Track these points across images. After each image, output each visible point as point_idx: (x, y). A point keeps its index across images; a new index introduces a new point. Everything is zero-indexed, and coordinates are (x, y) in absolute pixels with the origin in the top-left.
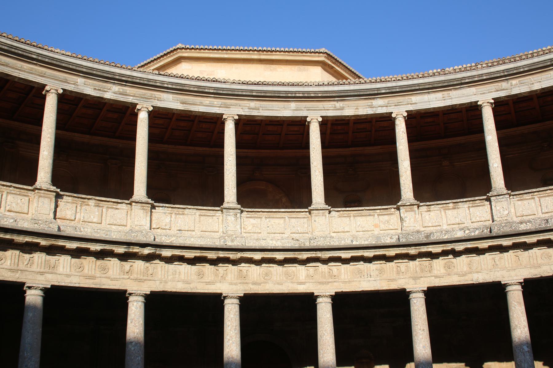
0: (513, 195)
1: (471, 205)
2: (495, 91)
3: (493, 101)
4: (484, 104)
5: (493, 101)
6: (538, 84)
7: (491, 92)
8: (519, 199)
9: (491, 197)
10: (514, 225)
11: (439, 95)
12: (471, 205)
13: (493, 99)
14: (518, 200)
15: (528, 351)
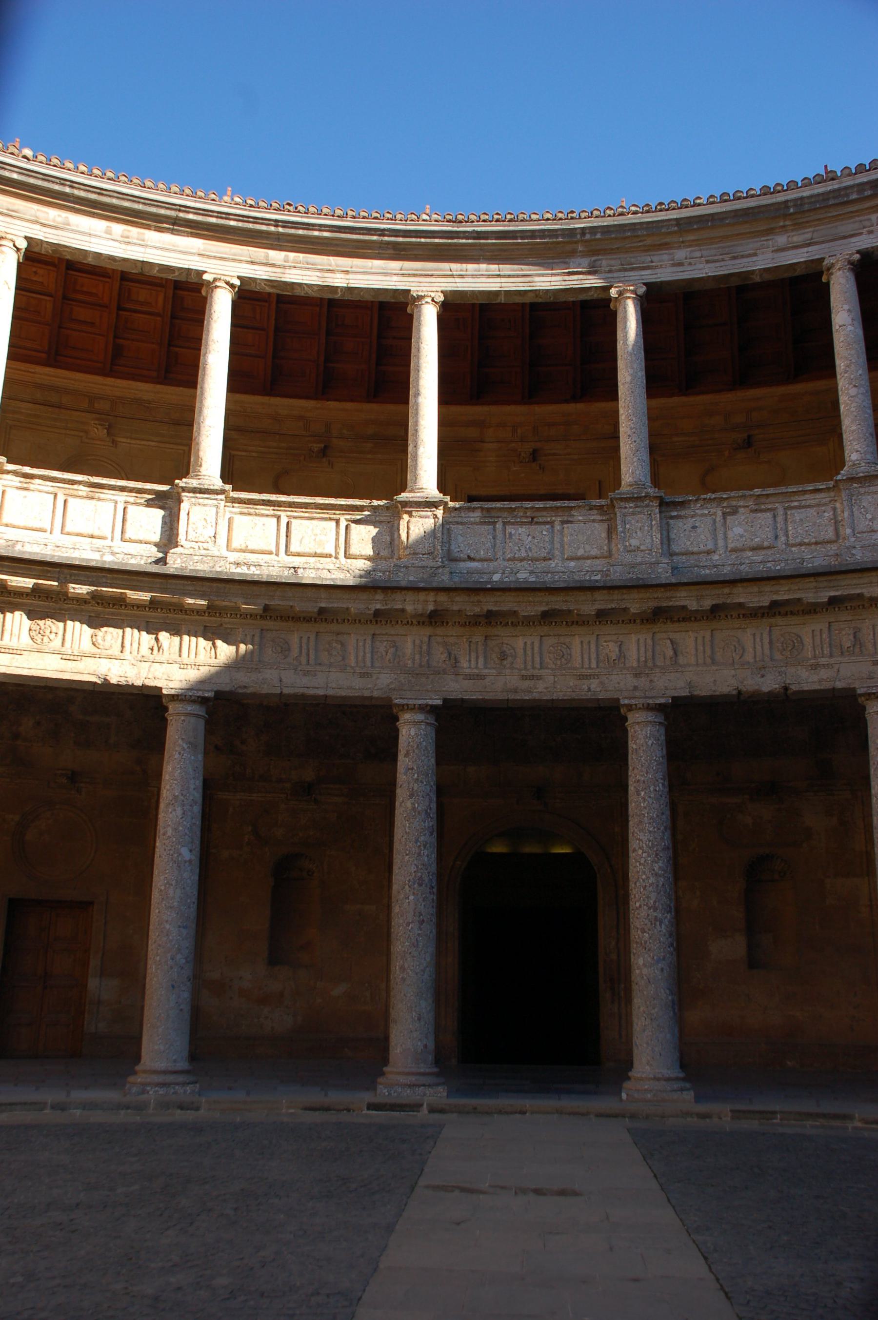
0: (234, 501)
1: (132, 500)
2: (247, 262)
3: (237, 282)
4: (218, 284)
5: (237, 282)
6: (342, 275)
7: (240, 261)
8: (245, 510)
9: (184, 489)
10: (222, 563)
11: (118, 229)
12: (132, 500)
13: (239, 277)
14: (242, 513)
15: (190, 861)
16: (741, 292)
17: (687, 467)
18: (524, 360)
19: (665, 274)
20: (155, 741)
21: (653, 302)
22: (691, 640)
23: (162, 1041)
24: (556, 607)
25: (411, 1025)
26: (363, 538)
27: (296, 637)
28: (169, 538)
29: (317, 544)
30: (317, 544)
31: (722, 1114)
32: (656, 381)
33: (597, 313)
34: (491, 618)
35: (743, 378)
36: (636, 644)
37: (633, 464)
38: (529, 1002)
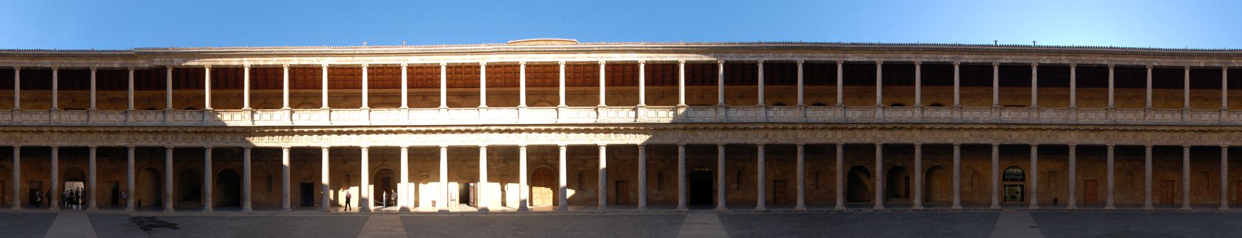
16: (743, 65)
17: (732, 100)
18: (700, 75)
19: (729, 59)
20: (637, 154)
21: (726, 65)
22: (730, 133)
23: (642, 202)
24: (707, 127)
25: (682, 199)
26: (671, 113)
27: (660, 133)
28: (636, 117)
29: (663, 115)
30: (663, 115)
31: (732, 211)
32: (726, 82)
33: (715, 66)
34: (695, 129)
35: (742, 84)
36: (720, 134)
37: (721, 99)
38: (701, 196)
